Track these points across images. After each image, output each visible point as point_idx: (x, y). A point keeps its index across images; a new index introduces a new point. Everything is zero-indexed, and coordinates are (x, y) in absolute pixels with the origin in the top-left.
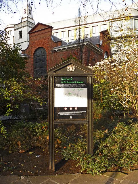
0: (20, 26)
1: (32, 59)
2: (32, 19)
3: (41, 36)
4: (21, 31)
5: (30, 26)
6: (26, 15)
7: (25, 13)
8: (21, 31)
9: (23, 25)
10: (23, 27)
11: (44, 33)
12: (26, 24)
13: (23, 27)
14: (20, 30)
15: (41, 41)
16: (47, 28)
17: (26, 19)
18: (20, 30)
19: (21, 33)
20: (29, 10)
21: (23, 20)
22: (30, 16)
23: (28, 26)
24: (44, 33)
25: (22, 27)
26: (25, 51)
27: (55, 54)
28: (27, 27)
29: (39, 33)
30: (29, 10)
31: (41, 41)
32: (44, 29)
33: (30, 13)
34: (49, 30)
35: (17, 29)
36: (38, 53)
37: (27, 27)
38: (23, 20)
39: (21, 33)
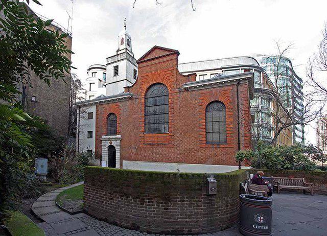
0: (116, 59)
1: (143, 101)
2: (131, 52)
3: (160, 66)
4: (118, 66)
5: (130, 60)
6: (124, 46)
7: (122, 43)
8: (118, 66)
9: (119, 58)
10: (120, 60)
11: (163, 62)
12: (124, 56)
13: (120, 60)
14: (115, 64)
15: (159, 74)
16: (169, 55)
17: (124, 51)
18: (115, 64)
19: (116, 68)
20: (128, 40)
21: (119, 53)
22: (129, 49)
23: (127, 59)
24: (163, 62)
25: (118, 61)
26: (130, 88)
27: (185, 93)
28: (125, 61)
29: (153, 62)
30: (128, 40)
31: (159, 74)
32: (164, 56)
33: (128, 45)
34: (174, 57)
35: (111, 63)
36: (155, 90)
37: (125, 61)
38: (119, 53)
39: (116, 68)
